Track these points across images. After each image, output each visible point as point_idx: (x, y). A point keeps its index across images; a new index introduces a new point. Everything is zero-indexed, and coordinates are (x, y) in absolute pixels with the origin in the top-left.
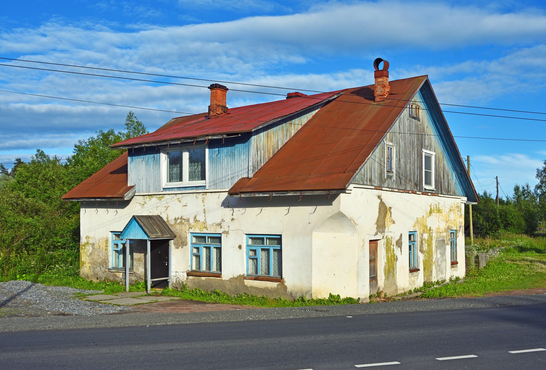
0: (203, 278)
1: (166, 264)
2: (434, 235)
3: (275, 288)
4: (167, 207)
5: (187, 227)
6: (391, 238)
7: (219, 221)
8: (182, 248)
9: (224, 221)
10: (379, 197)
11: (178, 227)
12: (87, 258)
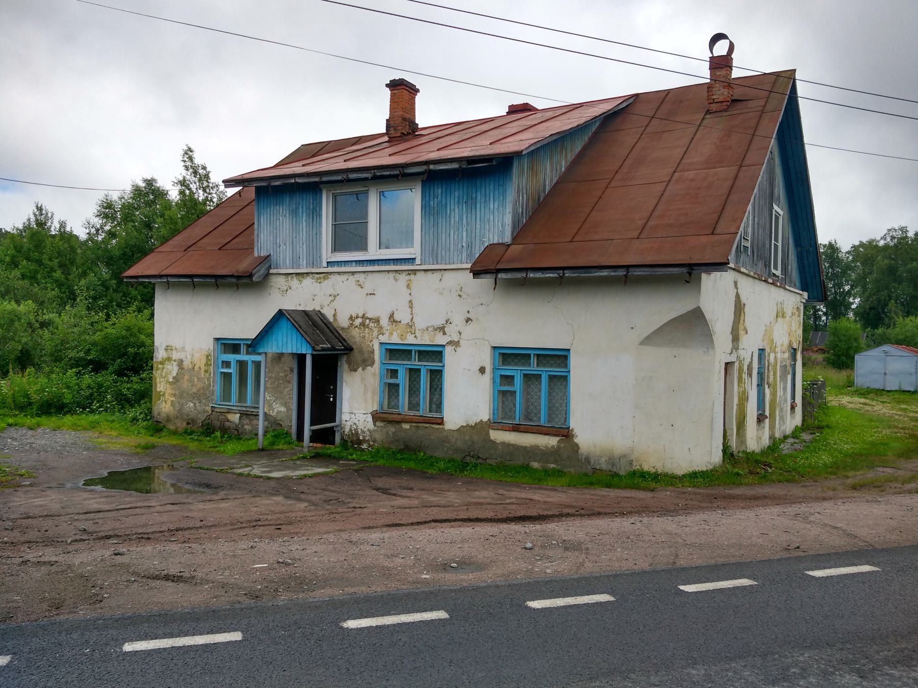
0: (406, 426)
1: (331, 399)
2: (779, 355)
3: (553, 447)
4: (335, 296)
5: (375, 333)
6: (744, 359)
7: (440, 322)
8: (363, 369)
9: (450, 323)
10: (736, 283)
11: (355, 333)
12: (168, 385)
